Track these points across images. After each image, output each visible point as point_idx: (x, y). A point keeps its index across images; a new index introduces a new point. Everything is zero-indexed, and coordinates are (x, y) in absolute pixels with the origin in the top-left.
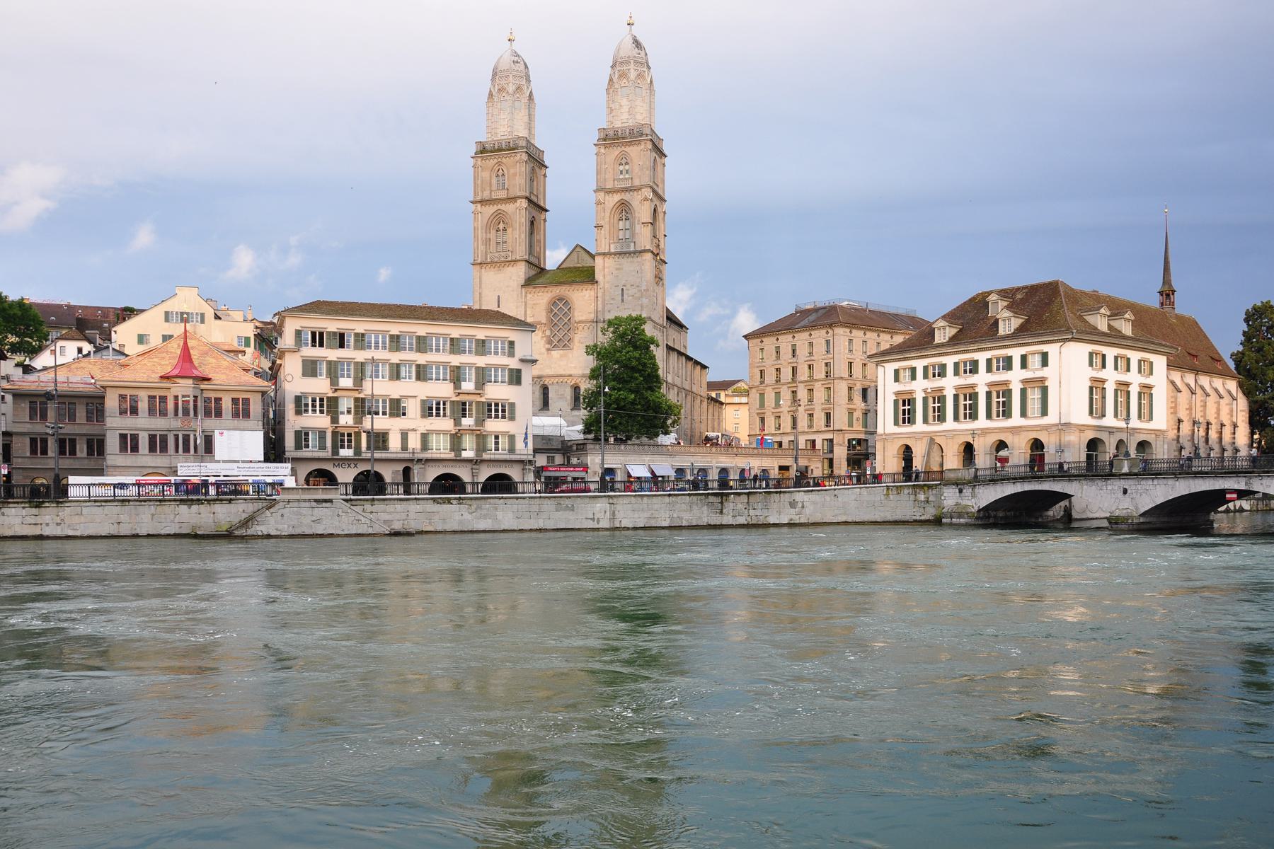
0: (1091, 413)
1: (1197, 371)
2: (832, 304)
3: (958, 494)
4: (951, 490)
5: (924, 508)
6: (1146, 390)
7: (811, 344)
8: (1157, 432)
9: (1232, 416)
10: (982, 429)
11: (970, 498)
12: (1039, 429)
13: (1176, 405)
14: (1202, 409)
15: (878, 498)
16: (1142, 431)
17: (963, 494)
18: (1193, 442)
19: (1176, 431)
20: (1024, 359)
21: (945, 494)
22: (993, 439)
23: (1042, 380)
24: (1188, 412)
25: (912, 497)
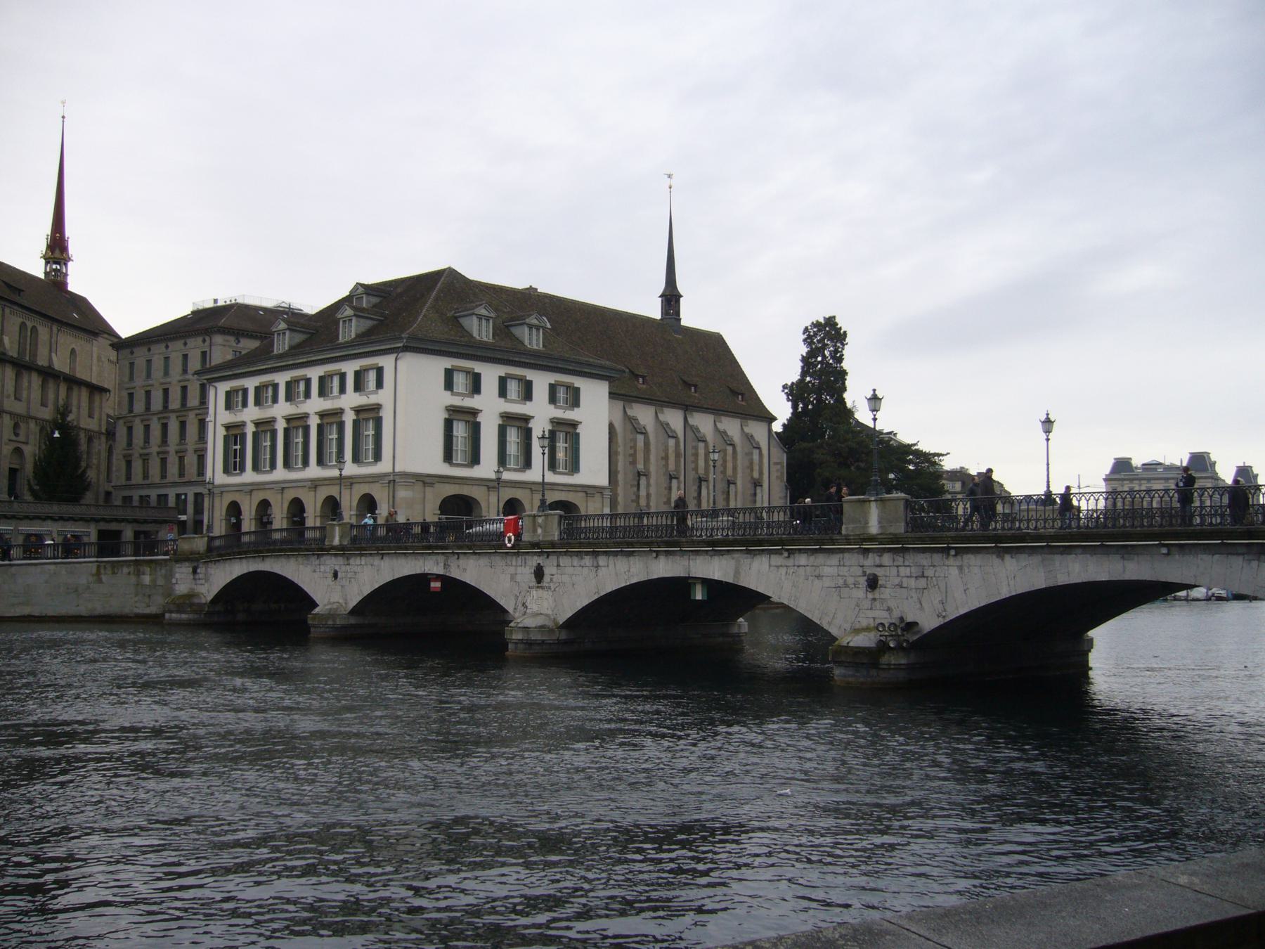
0: (448, 456)
1: (687, 408)
2: (233, 302)
3: (192, 577)
4: (184, 570)
5: (149, 596)
6: (566, 431)
7: (185, 357)
8: (588, 490)
9: (752, 470)
10: (312, 480)
11: (204, 581)
12: (370, 480)
13: (635, 451)
14: (692, 458)
15: (83, 581)
16: (556, 487)
17: (197, 577)
18: (638, 503)
19: (635, 489)
20: (359, 376)
21: (177, 576)
22: (323, 493)
23: (377, 408)
24: (663, 462)
25: (133, 579)
